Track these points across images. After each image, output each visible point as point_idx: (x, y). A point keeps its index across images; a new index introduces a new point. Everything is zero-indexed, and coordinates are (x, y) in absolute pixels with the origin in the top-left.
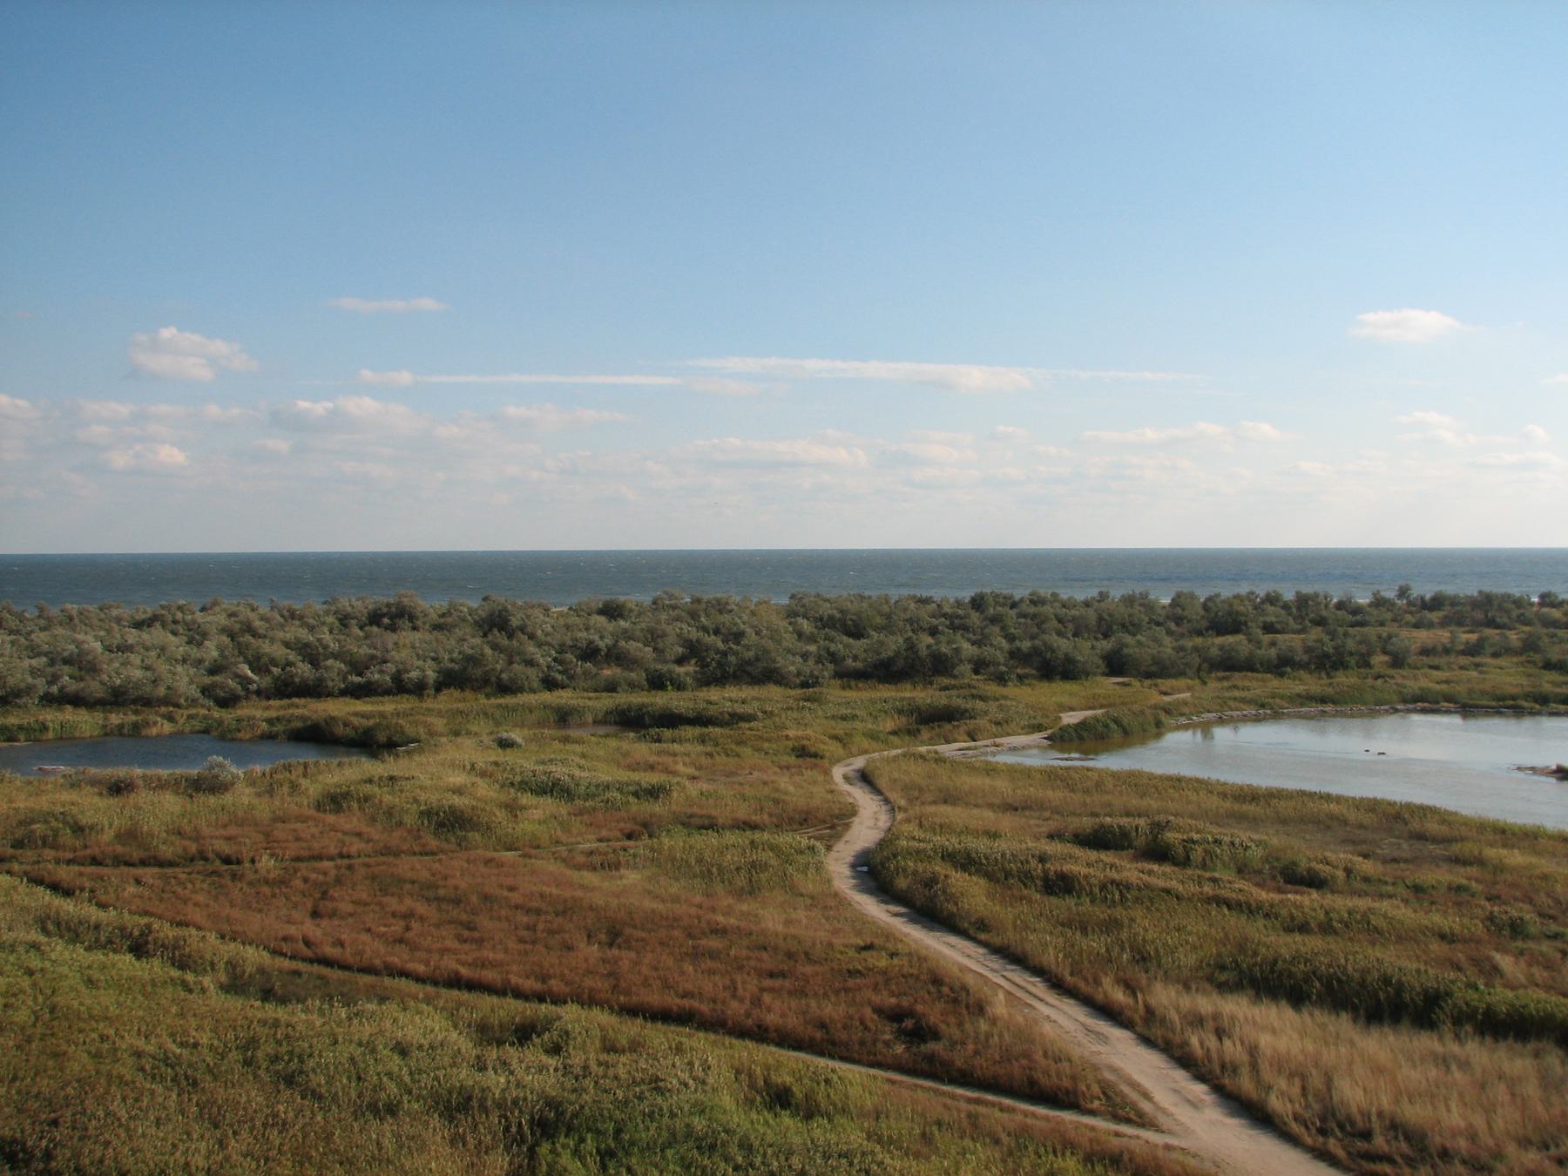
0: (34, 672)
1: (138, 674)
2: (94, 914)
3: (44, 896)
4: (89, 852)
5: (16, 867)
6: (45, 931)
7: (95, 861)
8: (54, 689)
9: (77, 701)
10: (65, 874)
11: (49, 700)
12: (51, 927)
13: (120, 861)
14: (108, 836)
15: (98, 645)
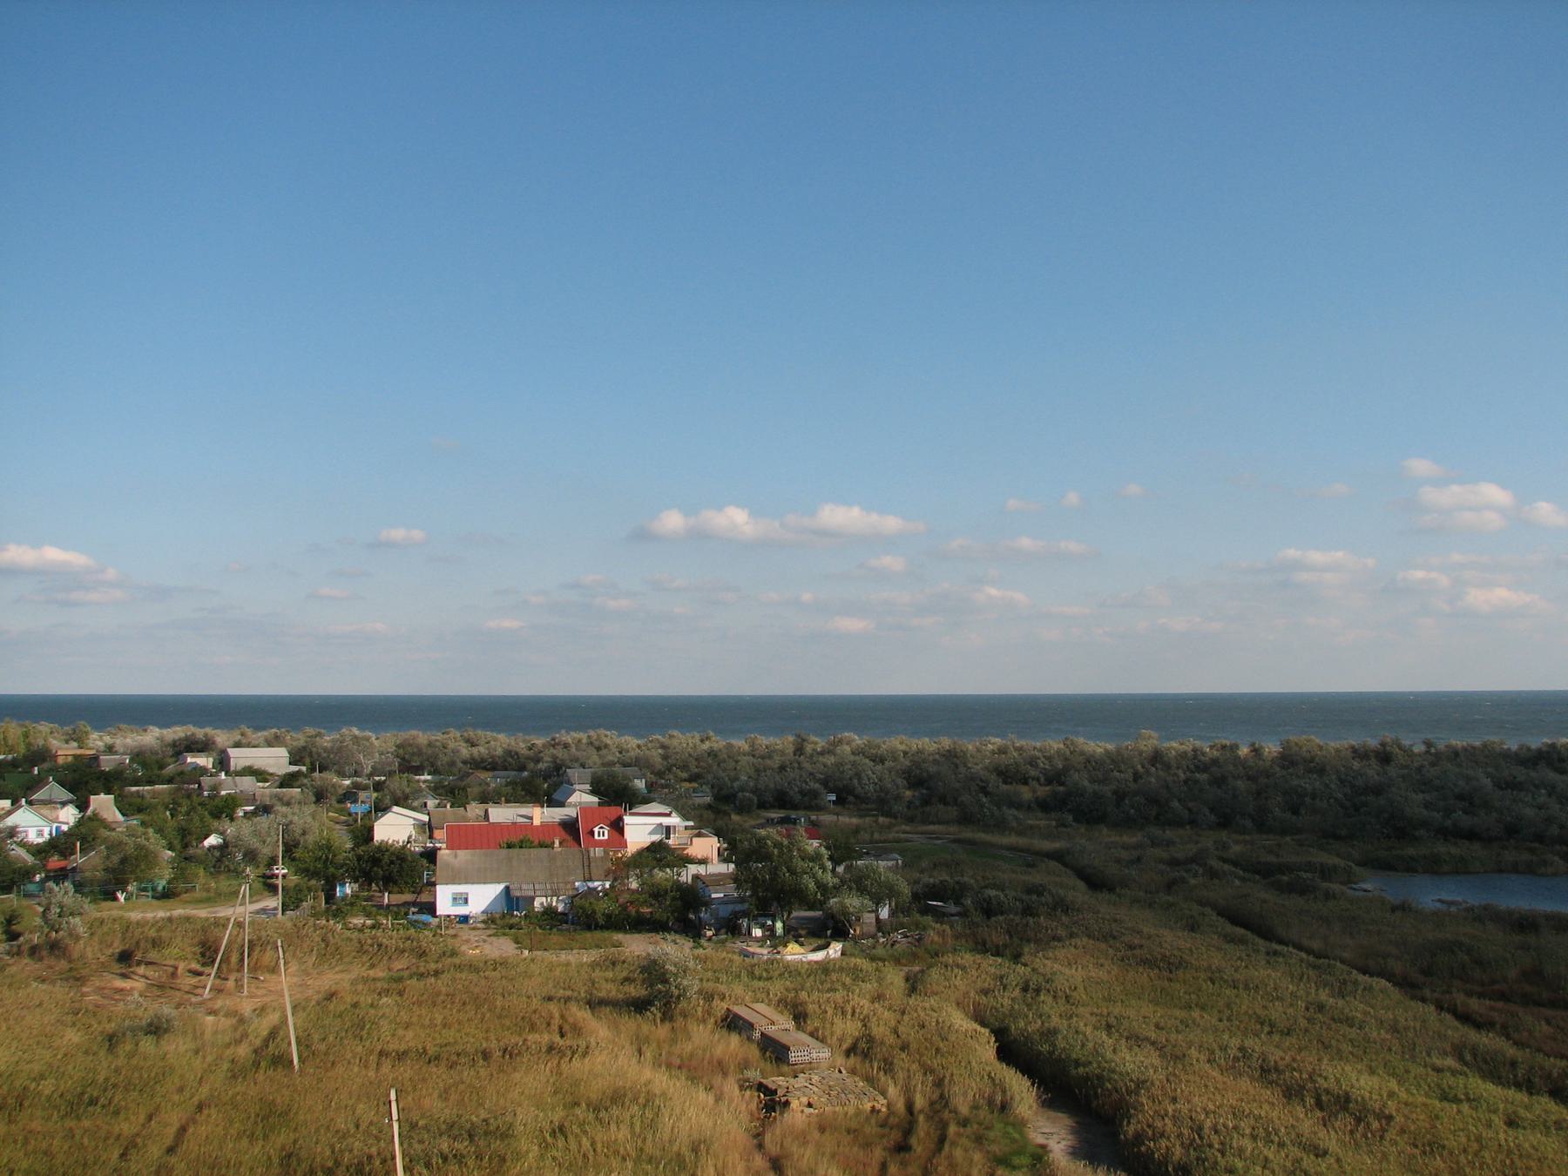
0: (1427, 805)
1: (1529, 812)
2: (1511, 1051)
3: (1458, 1031)
4: (1496, 987)
5: (1427, 993)
6: (1461, 1059)
7: (1503, 996)
8: (1448, 823)
9: (1471, 835)
10: (1475, 1004)
11: (1446, 834)
12: (1468, 1057)
13: (1528, 1001)
14: (1512, 973)
15: (1487, 782)
